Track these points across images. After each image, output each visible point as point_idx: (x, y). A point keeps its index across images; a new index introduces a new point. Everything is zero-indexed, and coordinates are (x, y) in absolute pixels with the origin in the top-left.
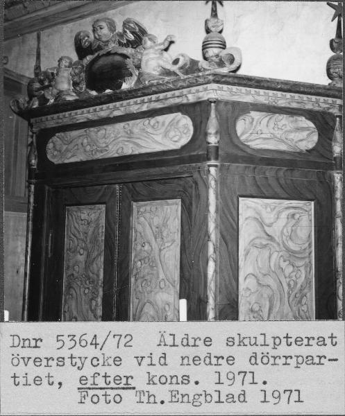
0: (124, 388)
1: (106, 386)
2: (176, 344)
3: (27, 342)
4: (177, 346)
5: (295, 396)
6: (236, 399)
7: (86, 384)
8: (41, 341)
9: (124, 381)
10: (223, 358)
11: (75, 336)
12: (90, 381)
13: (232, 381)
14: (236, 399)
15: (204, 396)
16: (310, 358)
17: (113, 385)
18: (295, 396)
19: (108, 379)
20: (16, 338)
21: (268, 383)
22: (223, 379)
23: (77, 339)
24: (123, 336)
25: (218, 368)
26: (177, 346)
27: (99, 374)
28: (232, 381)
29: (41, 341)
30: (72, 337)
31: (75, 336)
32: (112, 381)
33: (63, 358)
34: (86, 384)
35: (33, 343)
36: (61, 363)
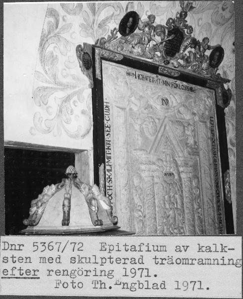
0: (32, 278)
1: (19, 276)
2: (149, 250)
3: (13, 247)
4: (150, 251)
5: (197, 285)
6: (159, 287)
7: (7, 274)
8: (23, 246)
9: (32, 273)
10: (128, 259)
11: (45, 243)
12: (10, 272)
13: (134, 274)
14: (159, 287)
15: (138, 284)
16: (133, 260)
17: (25, 276)
18: (197, 285)
19: (22, 272)
20: (6, 244)
21: (155, 274)
22: (128, 273)
23: (46, 245)
24: (77, 243)
25: (125, 266)
26: (150, 251)
27: (16, 268)
28: (134, 274)
29: (23, 246)
30: (43, 244)
31: (45, 243)
32: (24, 273)
33: (7, 258)
34: (7, 274)
35: (17, 247)
36: (6, 261)
